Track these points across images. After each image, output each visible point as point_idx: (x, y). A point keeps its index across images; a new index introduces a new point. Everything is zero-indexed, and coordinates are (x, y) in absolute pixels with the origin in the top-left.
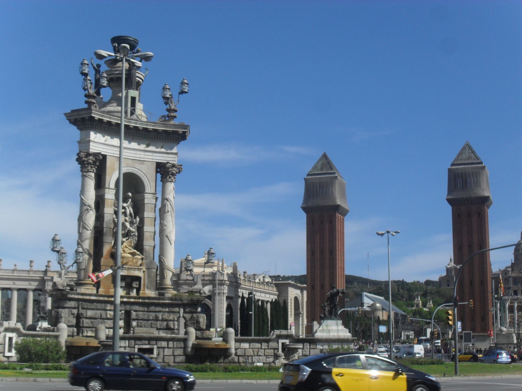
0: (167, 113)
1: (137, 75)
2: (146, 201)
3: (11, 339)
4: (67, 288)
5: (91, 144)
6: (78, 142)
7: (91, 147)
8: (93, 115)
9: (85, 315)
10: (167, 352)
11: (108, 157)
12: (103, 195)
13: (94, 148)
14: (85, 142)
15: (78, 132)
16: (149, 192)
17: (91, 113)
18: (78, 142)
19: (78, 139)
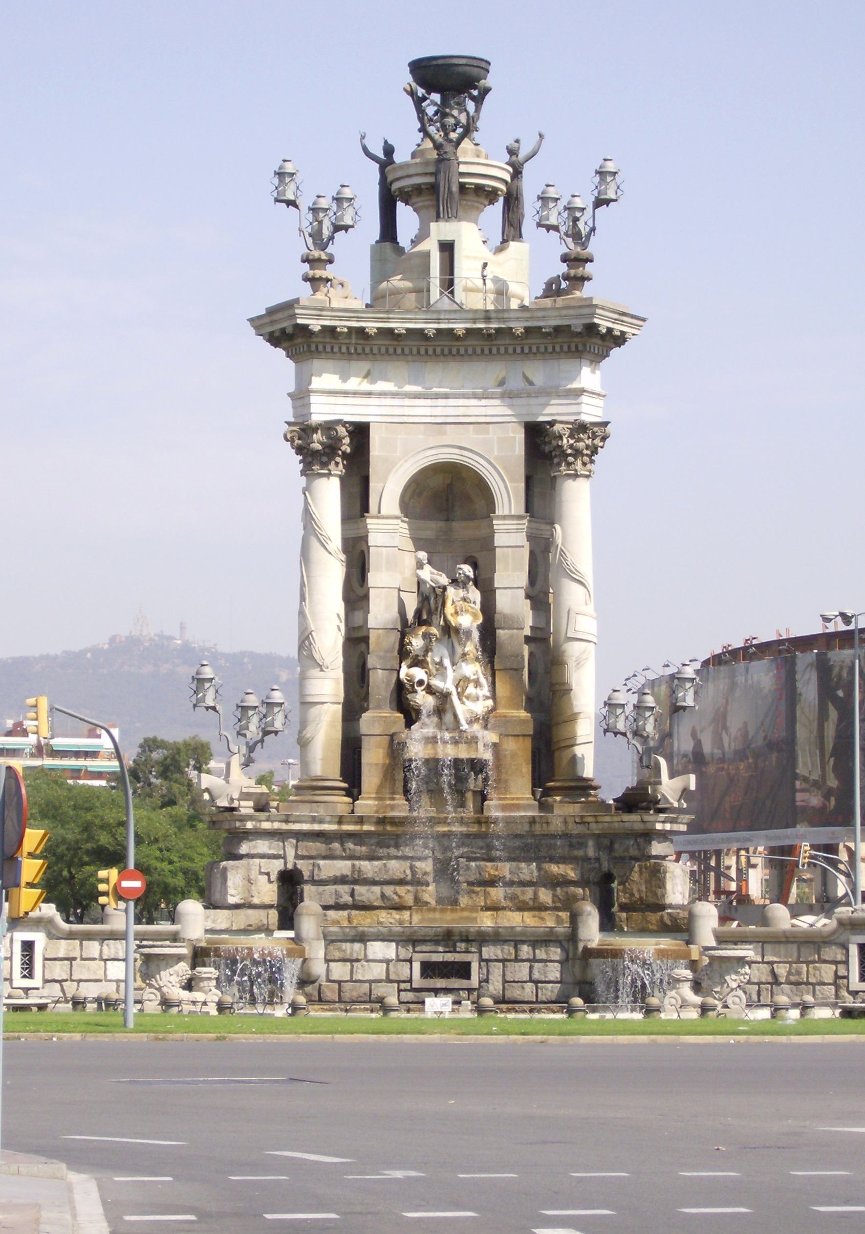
0: (563, 268)
1: (463, 169)
2: (499, 540)
3: (28, 947)
4: (243, 803)
5: (313, 399)
6: (290, 395)
7: (313, 409)
8: (299, 321)
9: (306, 875)
10: (522, 971)
11: (371, 424)
12: (365, 538)
13: (322, 410)
14: (301, 396)
15: (290, 365)
16: (506, 513)
17: (294, 316)
18: (290, 395)
19: (292, 388)
